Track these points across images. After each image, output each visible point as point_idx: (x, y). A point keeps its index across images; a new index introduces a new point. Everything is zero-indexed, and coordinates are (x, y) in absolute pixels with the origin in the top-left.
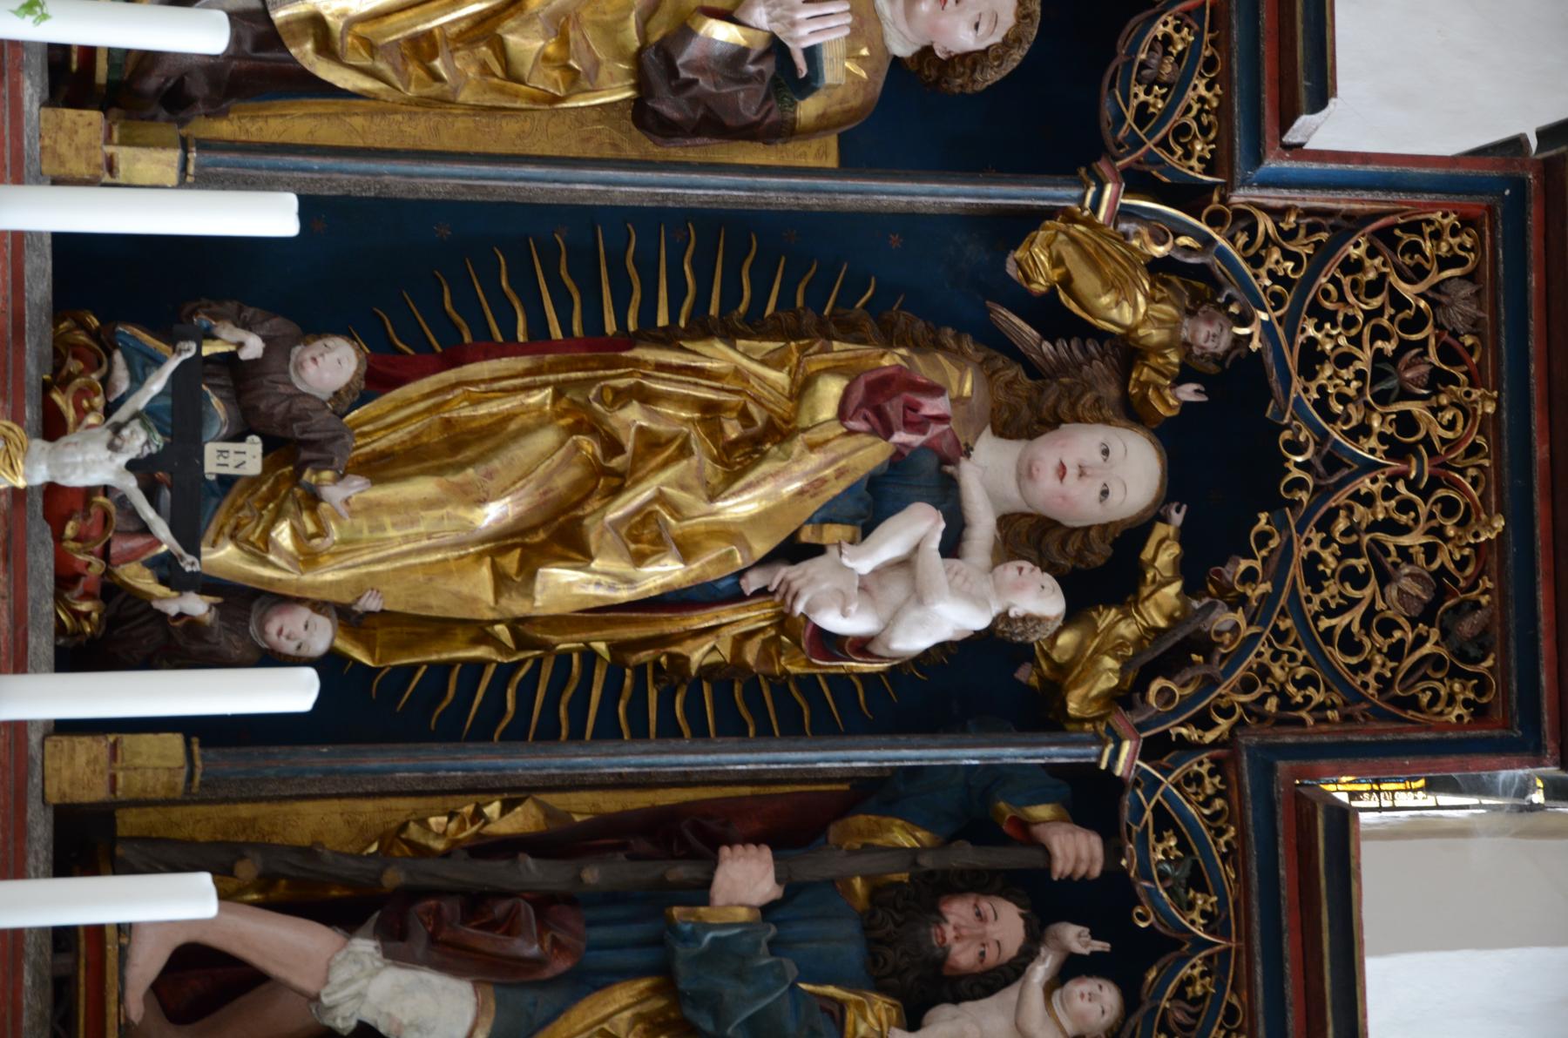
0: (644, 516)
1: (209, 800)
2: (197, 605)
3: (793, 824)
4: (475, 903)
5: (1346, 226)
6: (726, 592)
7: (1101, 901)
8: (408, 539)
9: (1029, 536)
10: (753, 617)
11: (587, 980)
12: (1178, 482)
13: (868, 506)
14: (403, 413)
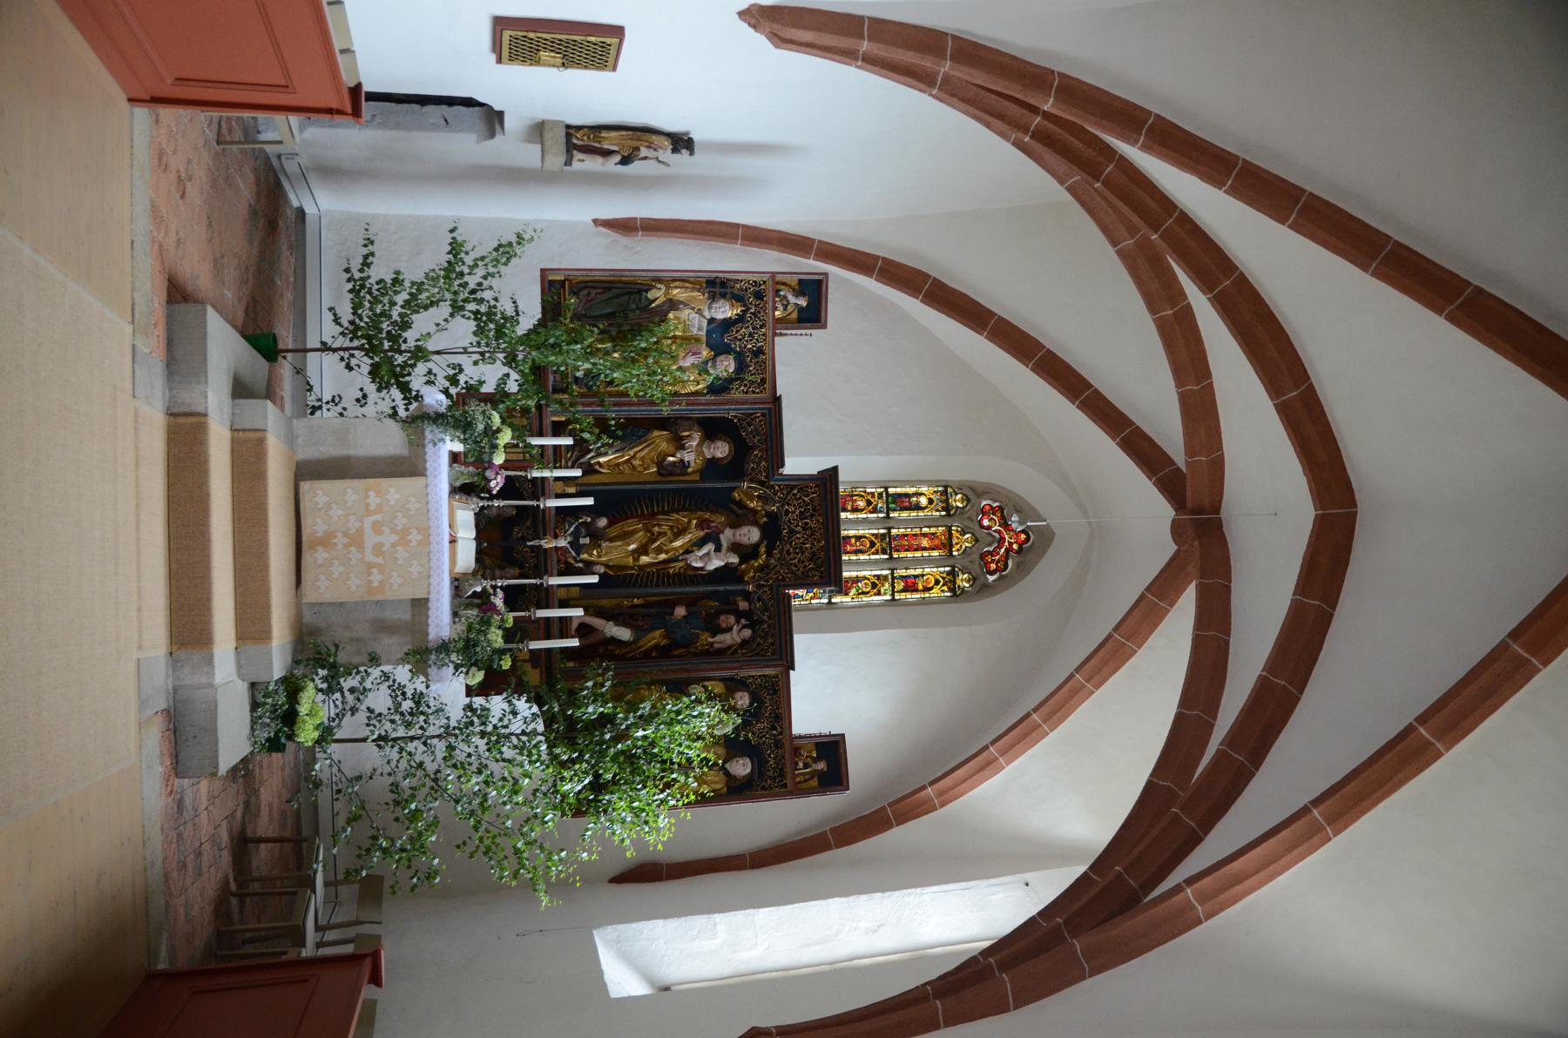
1: (582, 596)
5: (793, 487)
6: (675, 560)
7: (747, 614)
8: (617, 553)
9: (736, 547)
12: (763, 537)
13: (701, 543)
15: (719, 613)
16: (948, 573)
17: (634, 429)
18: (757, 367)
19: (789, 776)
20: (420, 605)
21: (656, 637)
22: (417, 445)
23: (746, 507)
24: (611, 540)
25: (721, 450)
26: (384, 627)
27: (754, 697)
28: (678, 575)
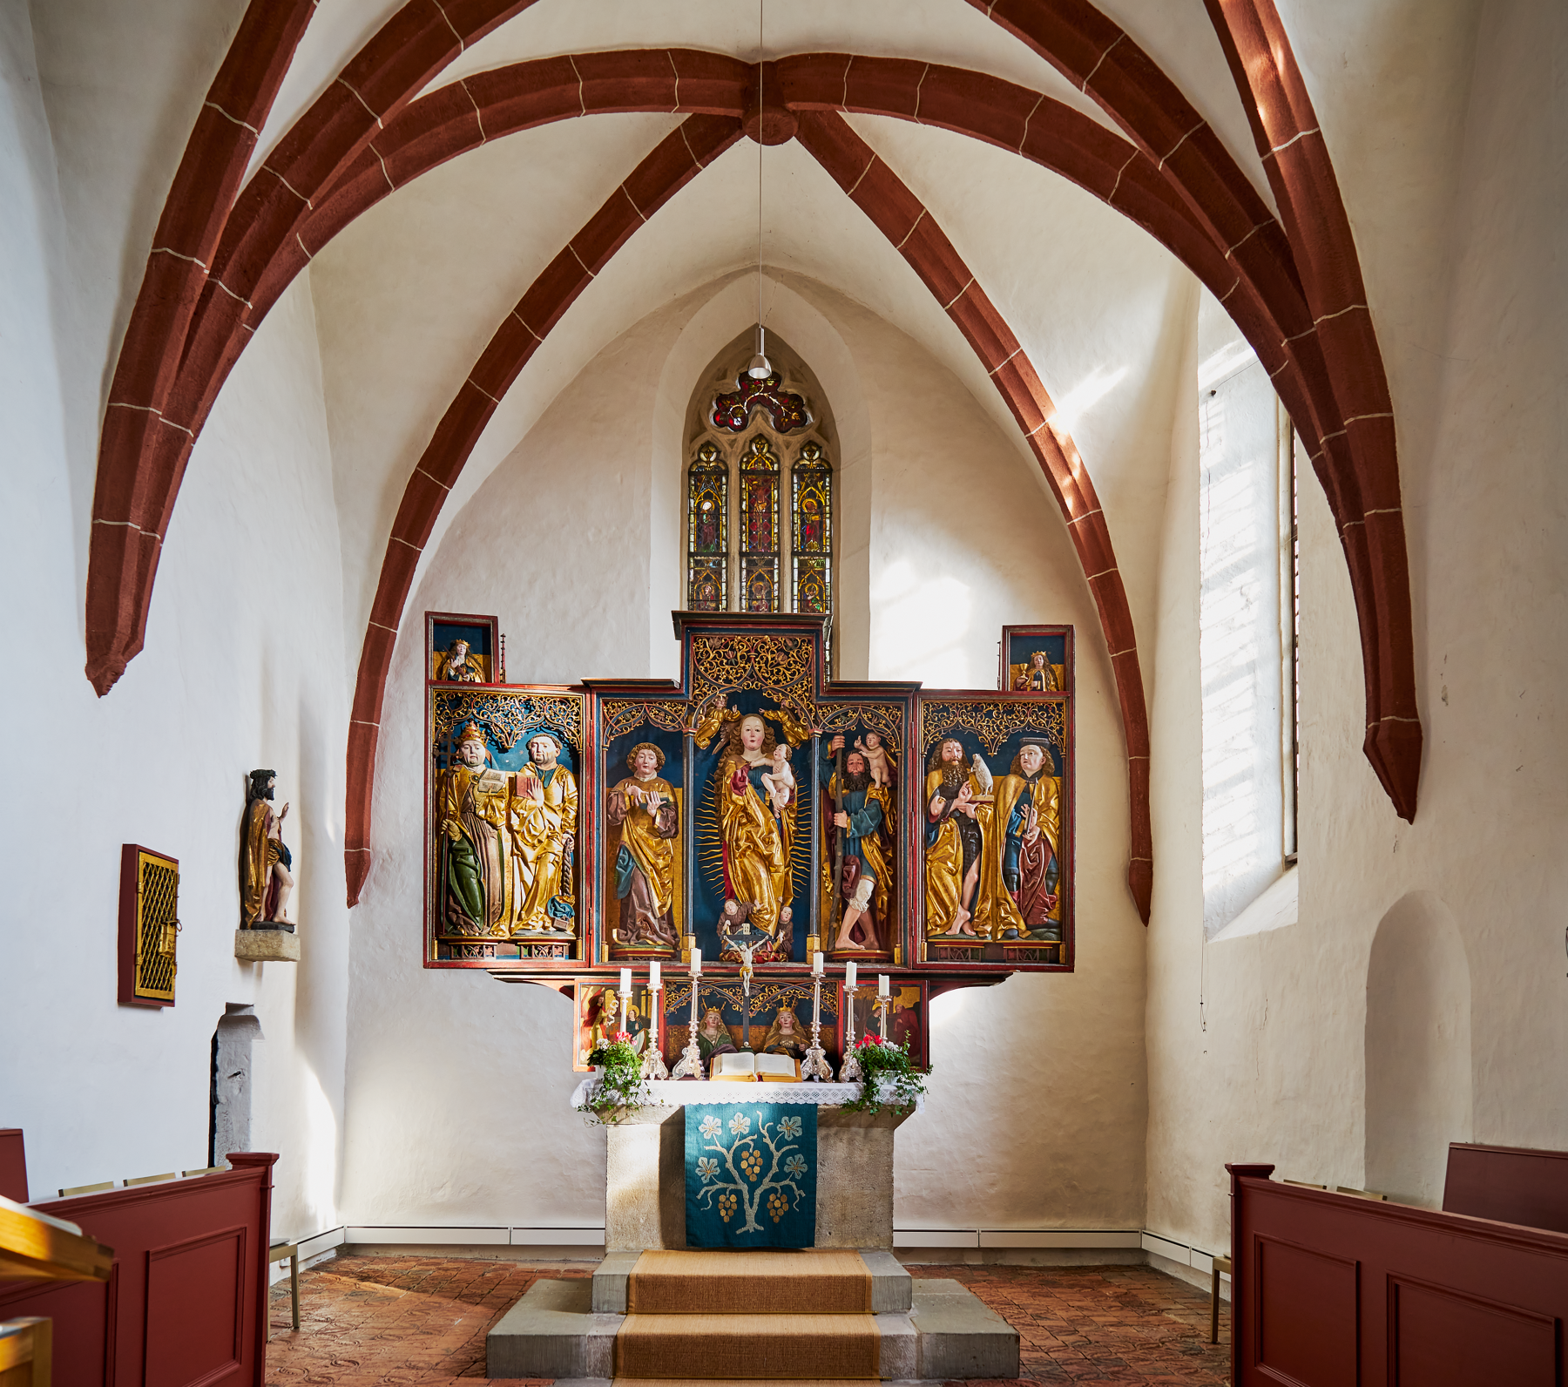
0: (763, 841)
2: (781, 934)
3: (831, 807)
4: (844, 879)
7: (850, 737)
9: (767, 748)
10: (784, 814)
11: (861, 855)
12: (754, 711)
13: (760, 788)
14: (741, 892)
15: (845, 773)
16: (801, 479)
19: (1047, 699)
21: (871, 851)
23: (718, 733)
24: (752, 898)
25: (648, 758)
27: (947, 737)
28: (797, 820)
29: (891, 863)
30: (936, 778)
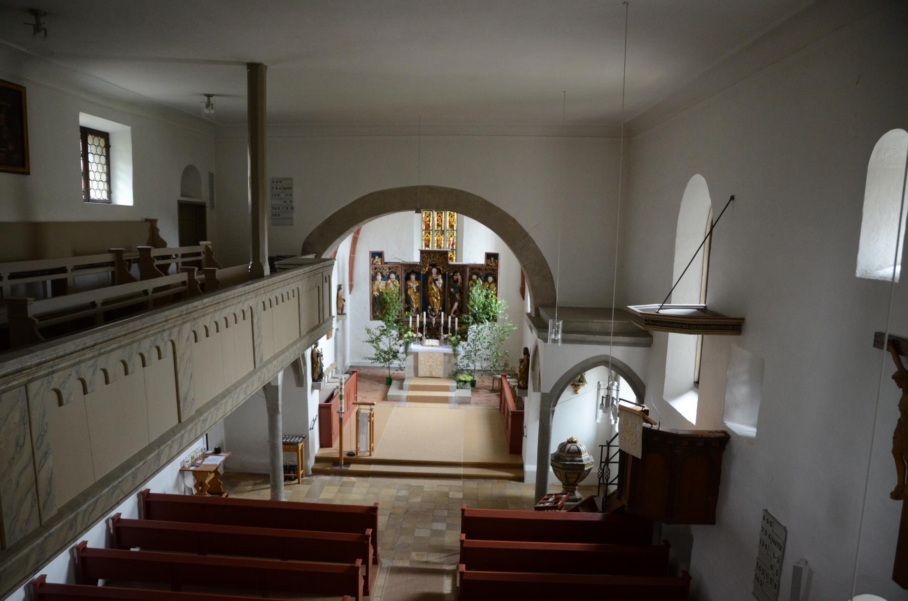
17: (408, 300)
18: (394, 268)
20: (445, 354)
21: (457, 296)
22: (412, 353)
25: (413, 277)
26: (449, 361)
29: (462, 298)
30: (471, 282)
